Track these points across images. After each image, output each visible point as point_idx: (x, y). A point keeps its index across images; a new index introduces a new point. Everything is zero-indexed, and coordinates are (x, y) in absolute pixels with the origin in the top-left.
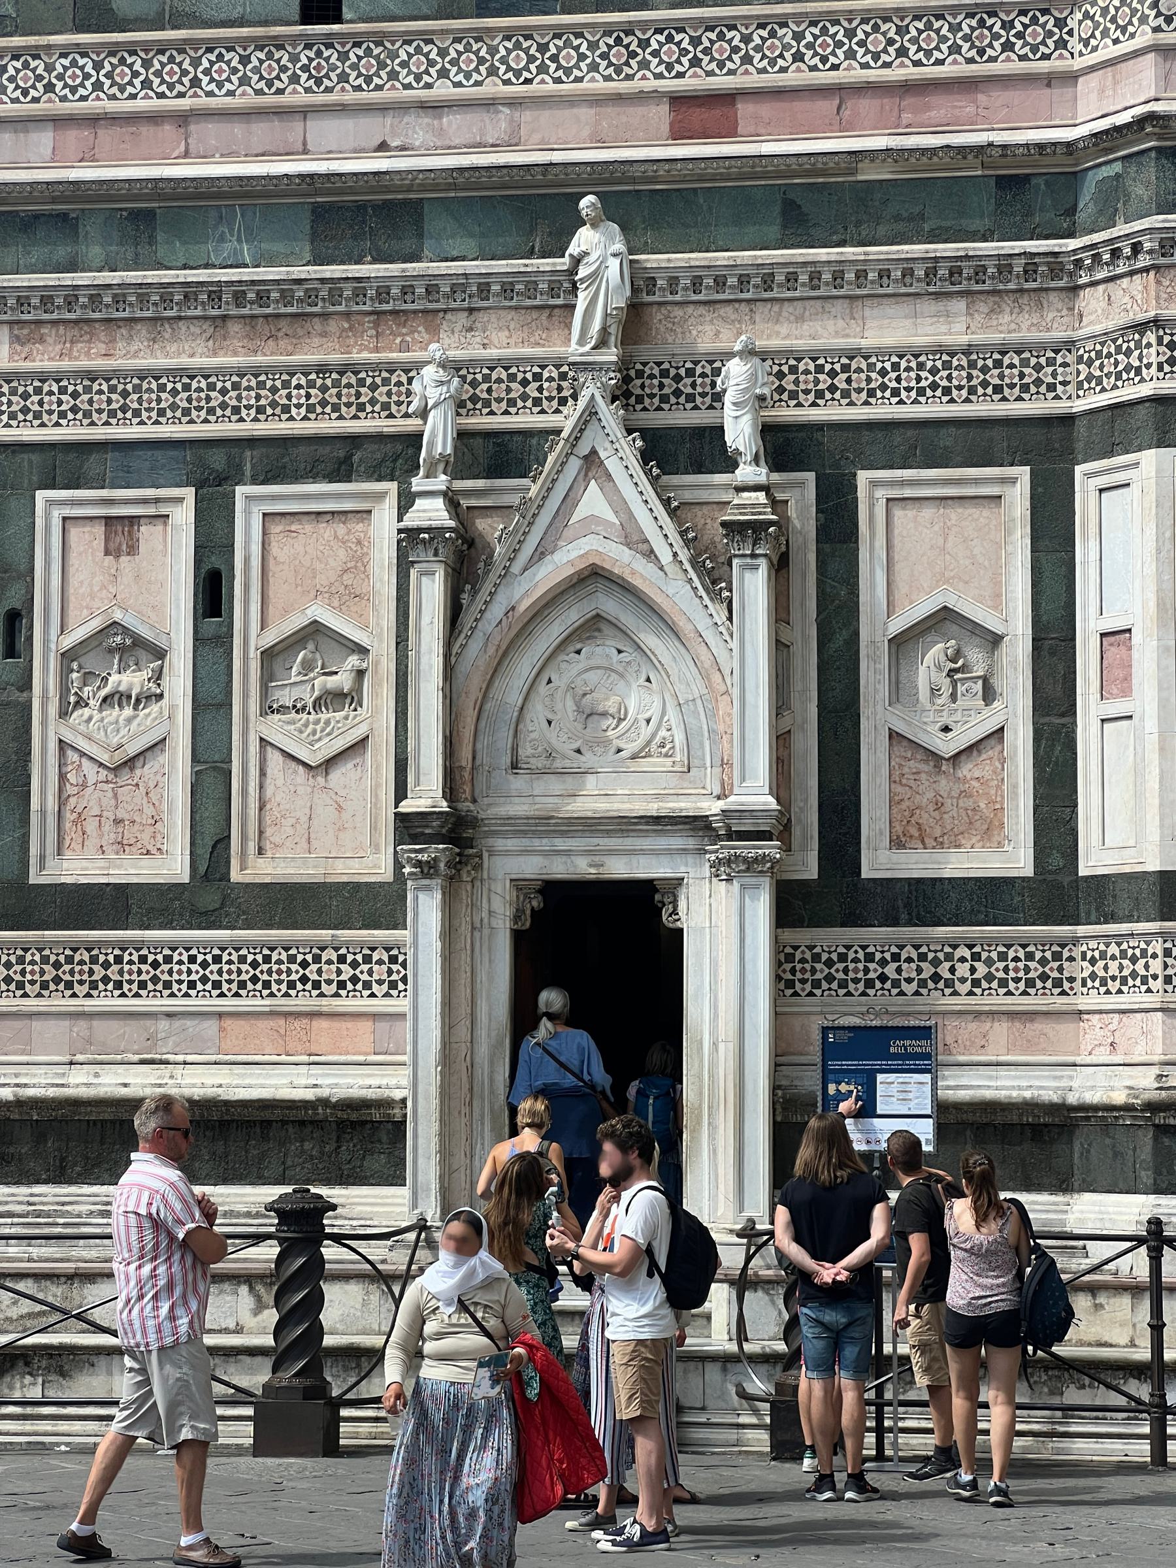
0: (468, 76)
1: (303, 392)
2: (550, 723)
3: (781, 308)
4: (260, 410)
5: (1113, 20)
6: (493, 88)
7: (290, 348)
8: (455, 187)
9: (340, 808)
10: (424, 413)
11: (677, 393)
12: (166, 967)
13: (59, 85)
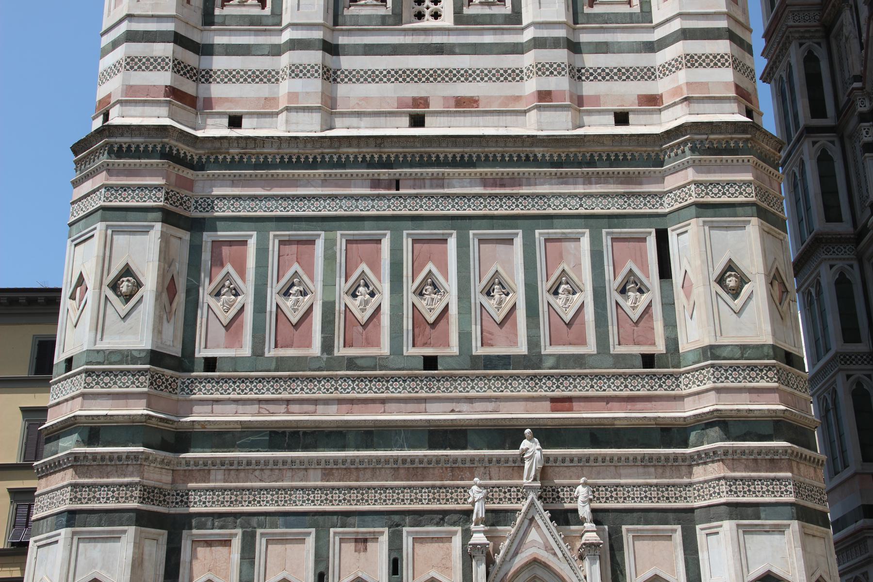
4: (412, 500)
5: (697, 379)
8: (478, 426)
10: (473, 503)
13: (340, 388)
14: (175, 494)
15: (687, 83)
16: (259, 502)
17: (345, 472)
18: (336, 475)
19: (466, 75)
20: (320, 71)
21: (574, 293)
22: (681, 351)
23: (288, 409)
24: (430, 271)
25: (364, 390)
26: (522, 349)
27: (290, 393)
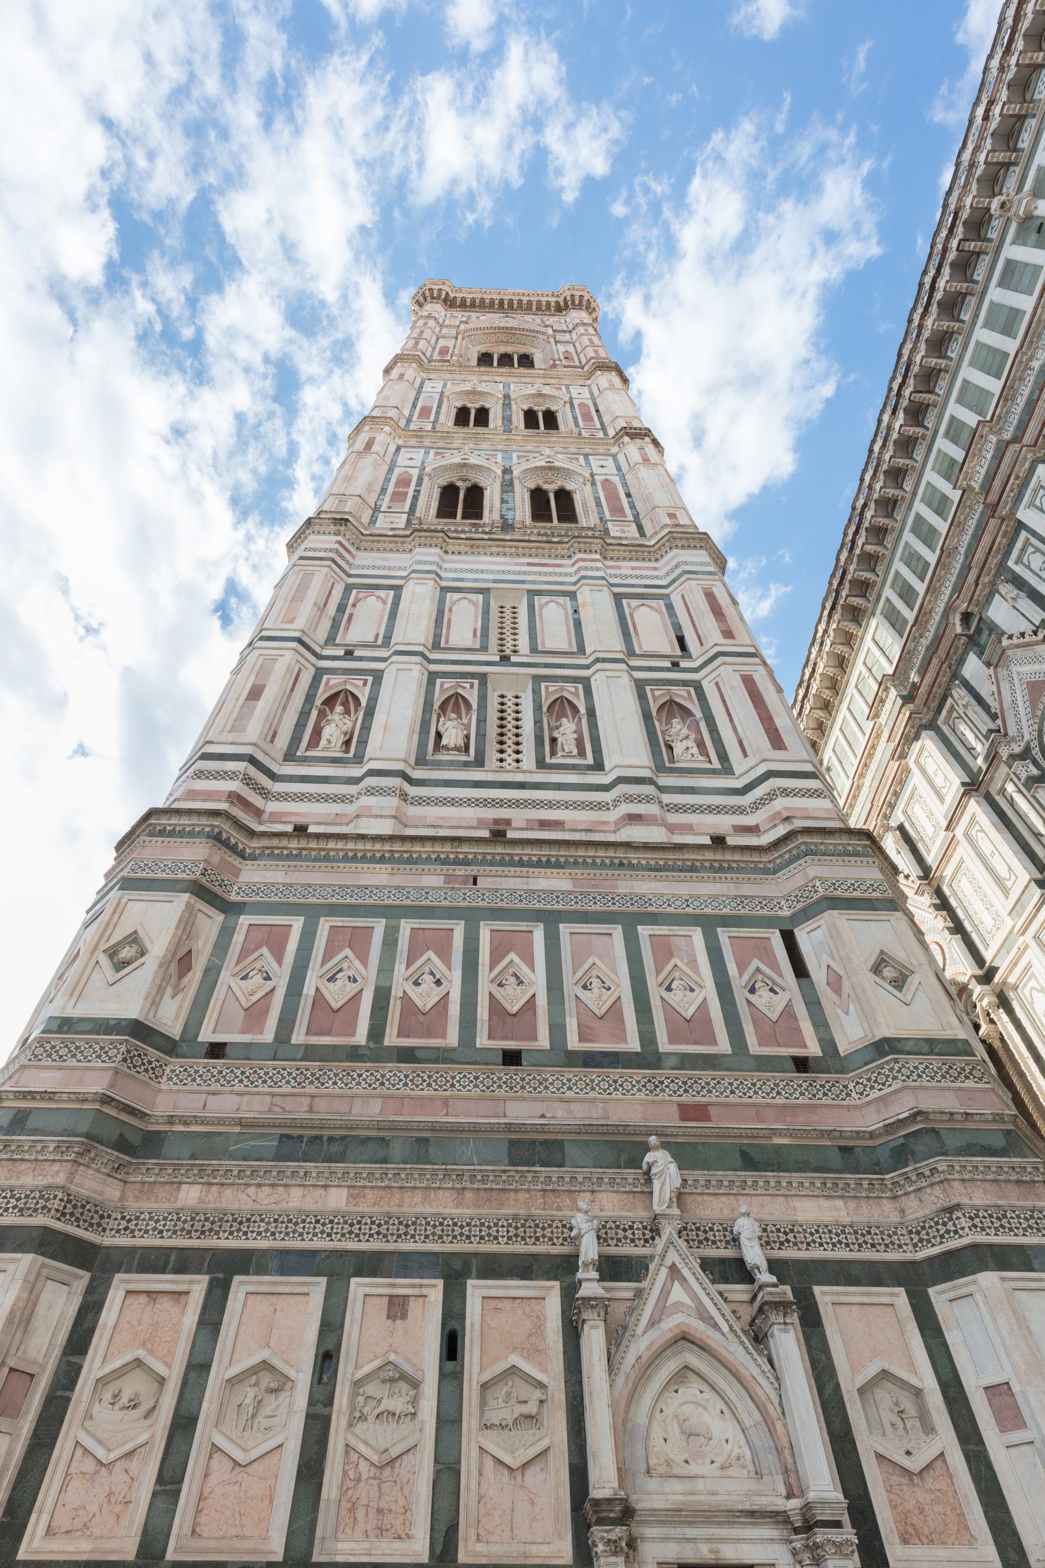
0: (582, 1090)
2: (665, 1440)
4: (482, 1238)
6: (592, 1094)
9: (532, 1503)
11: (707, 1239)
13: (387, 1083)
15: (785, 808)
16: (245, 1233)
18: (369, 1197)
19: (550, 805)
20: (398, 792)
21: (692, 990)
22: (842, 1054)
23: (311, 1107)
24: (512, 961)
26: (633, 1044)
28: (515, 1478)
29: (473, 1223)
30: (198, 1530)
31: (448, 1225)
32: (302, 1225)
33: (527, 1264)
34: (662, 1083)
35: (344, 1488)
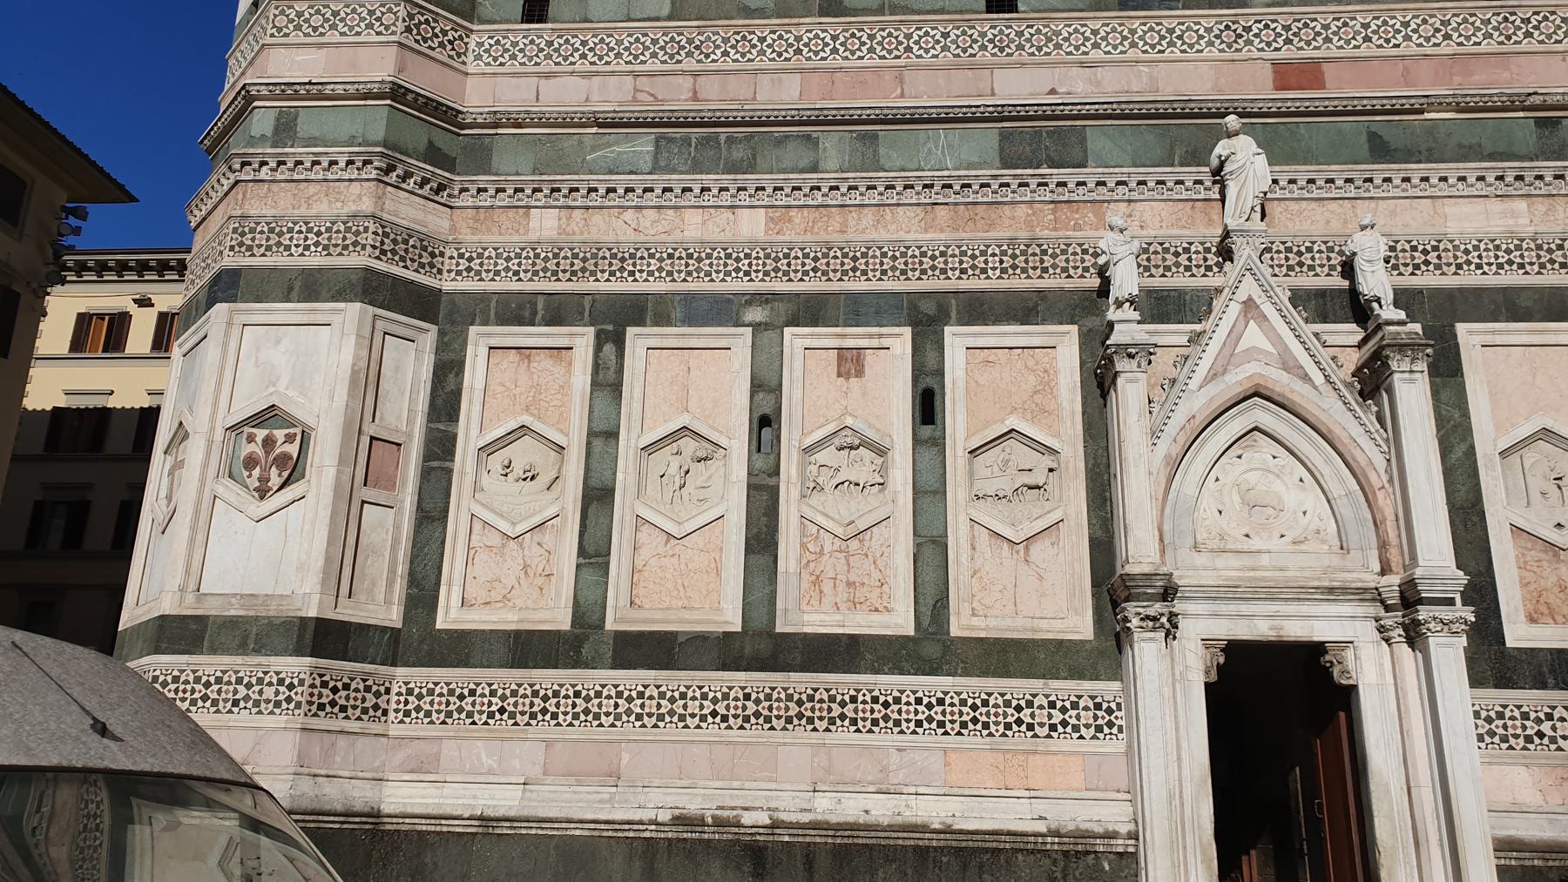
0: (1115, 47)
1: (997, 259)
2: (1220, 512)
3: (1377, 205)
4: (963, 271)
6: (1132, 54)
7: (986, 228)
9: (1041, 578)
11: (1301, 264)
12: (896, 707)
13: (806, 50)
14: (455, 255)
16: (632, 273)
17: (814, 214)
18: (797, 221)
23: (695, 92)
25: (858, 53)
27: (699, 61)
28: (1018, 552)
29: (950, 252)
30: (637, 601)
31: (914, 256)
32: (708, 262)
33: (1030, 304)
34: (1248, 29)
35: (804, 561)
